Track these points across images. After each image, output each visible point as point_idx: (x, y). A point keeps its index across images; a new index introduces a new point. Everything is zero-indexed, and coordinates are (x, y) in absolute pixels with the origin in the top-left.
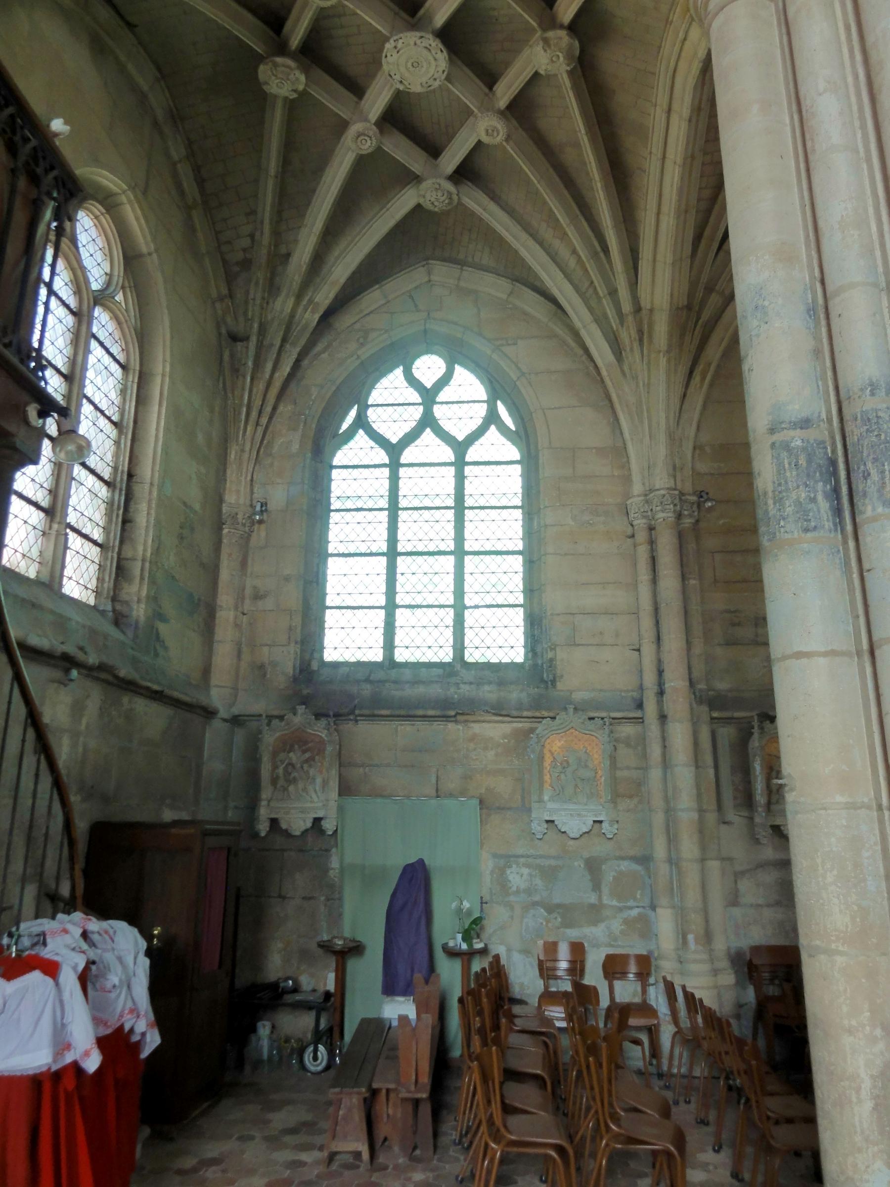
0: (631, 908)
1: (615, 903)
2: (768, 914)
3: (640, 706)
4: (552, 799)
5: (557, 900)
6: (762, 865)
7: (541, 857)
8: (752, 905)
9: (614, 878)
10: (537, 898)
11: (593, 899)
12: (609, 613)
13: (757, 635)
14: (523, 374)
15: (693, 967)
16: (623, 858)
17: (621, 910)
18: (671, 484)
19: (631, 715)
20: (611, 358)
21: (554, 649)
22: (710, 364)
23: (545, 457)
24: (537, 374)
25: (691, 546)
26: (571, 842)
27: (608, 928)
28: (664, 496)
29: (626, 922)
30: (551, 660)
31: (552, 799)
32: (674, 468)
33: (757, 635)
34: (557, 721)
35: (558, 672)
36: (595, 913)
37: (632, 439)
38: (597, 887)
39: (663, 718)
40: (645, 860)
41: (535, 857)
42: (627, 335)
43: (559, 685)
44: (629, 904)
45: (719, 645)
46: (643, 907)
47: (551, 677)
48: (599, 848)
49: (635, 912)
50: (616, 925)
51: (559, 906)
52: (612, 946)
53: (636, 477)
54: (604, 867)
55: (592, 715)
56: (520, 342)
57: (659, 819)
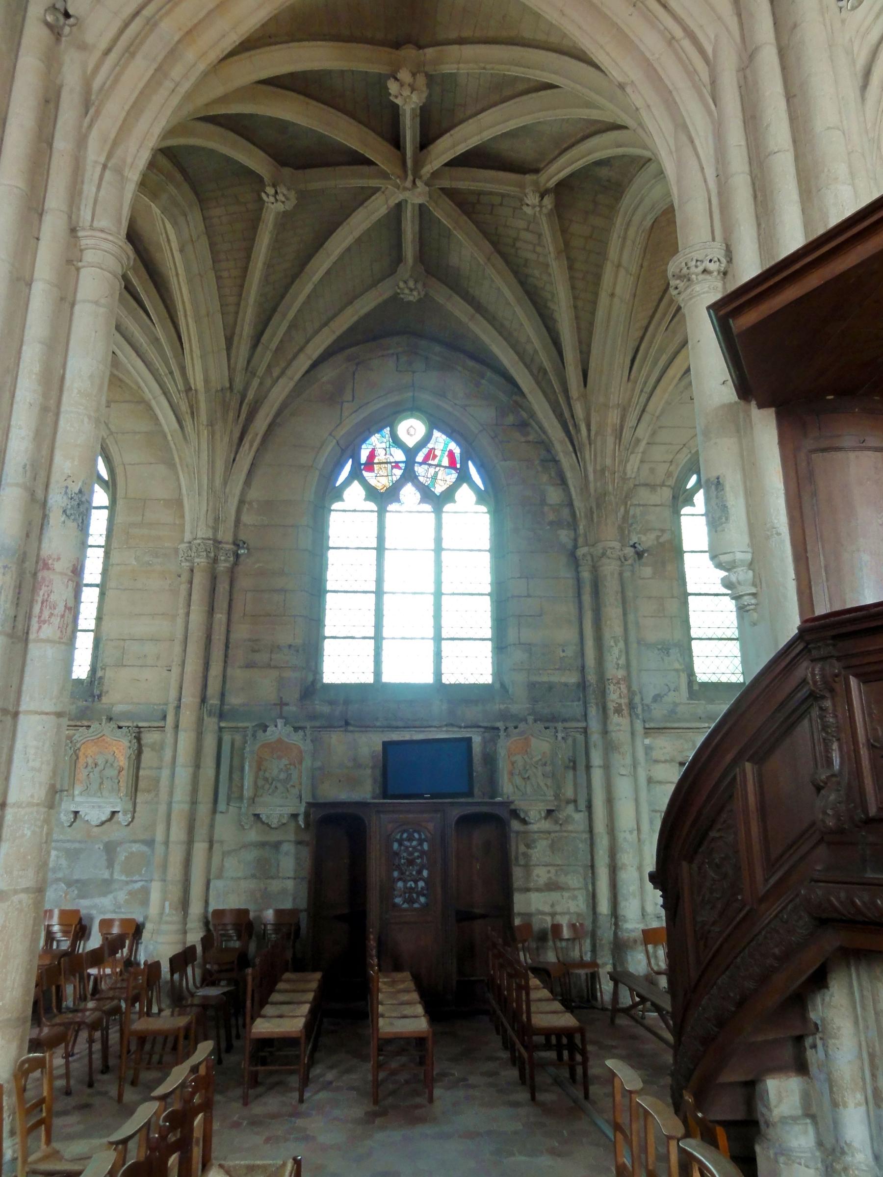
0: (136, 882)
1: (123, 878)
2: (251, 884)
3: (164, 718)
4: (81, 794)
5: (75, 877)
6: (245, 846)
7: (68, 841)
8: (232, 878)
9: (126, 857)
10: (60, 875)
11: (106, 875)
12: (154, 640)
13: (271, 660)
14: (112, 433)
15: (164, 927)
16: (135, 842)
17: (127, 883)
18: (210, 534)
19: (156, 724)
20: (176, 425)
21: (105, 669)
22: (257, 435)
23: (120, 503)
24: (123, 433)
25: (223, 587)
26: (95, 829)
27: (115, 898)
28: (199, 545)
29: (130, 893)
30: (101, 678)
31: (81, 794)
32: (217, 520)
33: (271, 660)
34: (91, 730)
35: (105, 688)
36: (106, 887)
37: (188, 495)
38: (110, 865)
39: (177, 727)
40: (150, 843)
41: (63, 841)
42: (184, 407)
43: (104, 700)
44: (134, 879)
45: (240, 667)
46: (146, 881)
47: (98, 692)
48: (115, 833)
49: (138, 885)
50: (122, 896)
51: (77, 881)
52: (115, 912)
53: (188, 527)
54: (118, 849)
55: (121, 724)
56: (112, 405)
57: (162, 808)
